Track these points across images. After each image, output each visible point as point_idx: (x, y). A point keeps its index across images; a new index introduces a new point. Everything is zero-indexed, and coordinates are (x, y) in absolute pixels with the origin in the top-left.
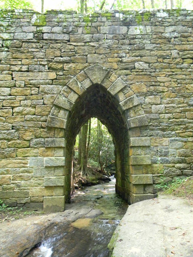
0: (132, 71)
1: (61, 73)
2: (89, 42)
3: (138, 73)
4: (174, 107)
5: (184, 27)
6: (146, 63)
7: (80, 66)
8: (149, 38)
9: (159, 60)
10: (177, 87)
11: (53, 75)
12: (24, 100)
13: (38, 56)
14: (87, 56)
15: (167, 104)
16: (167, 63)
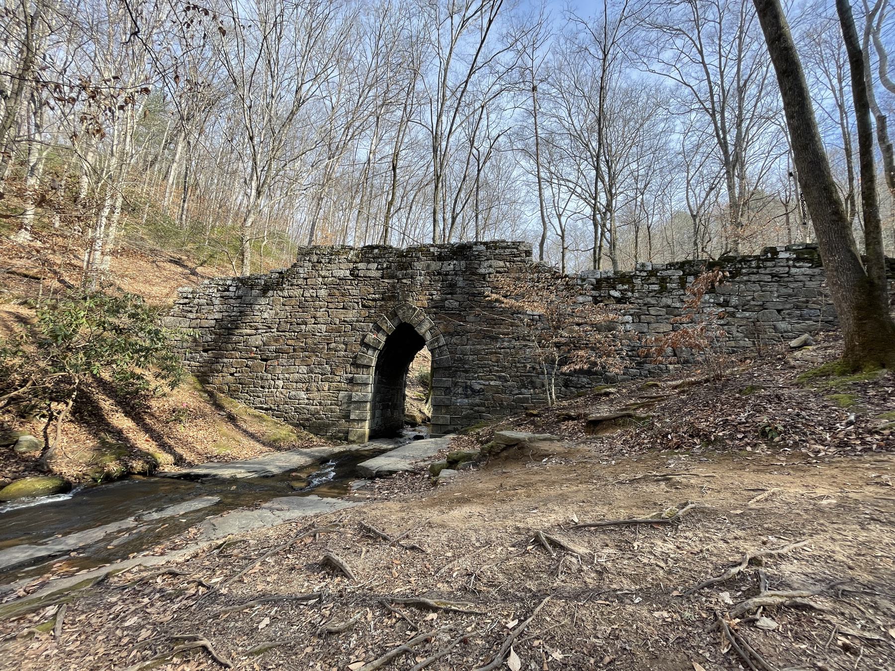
6: (457, 301)
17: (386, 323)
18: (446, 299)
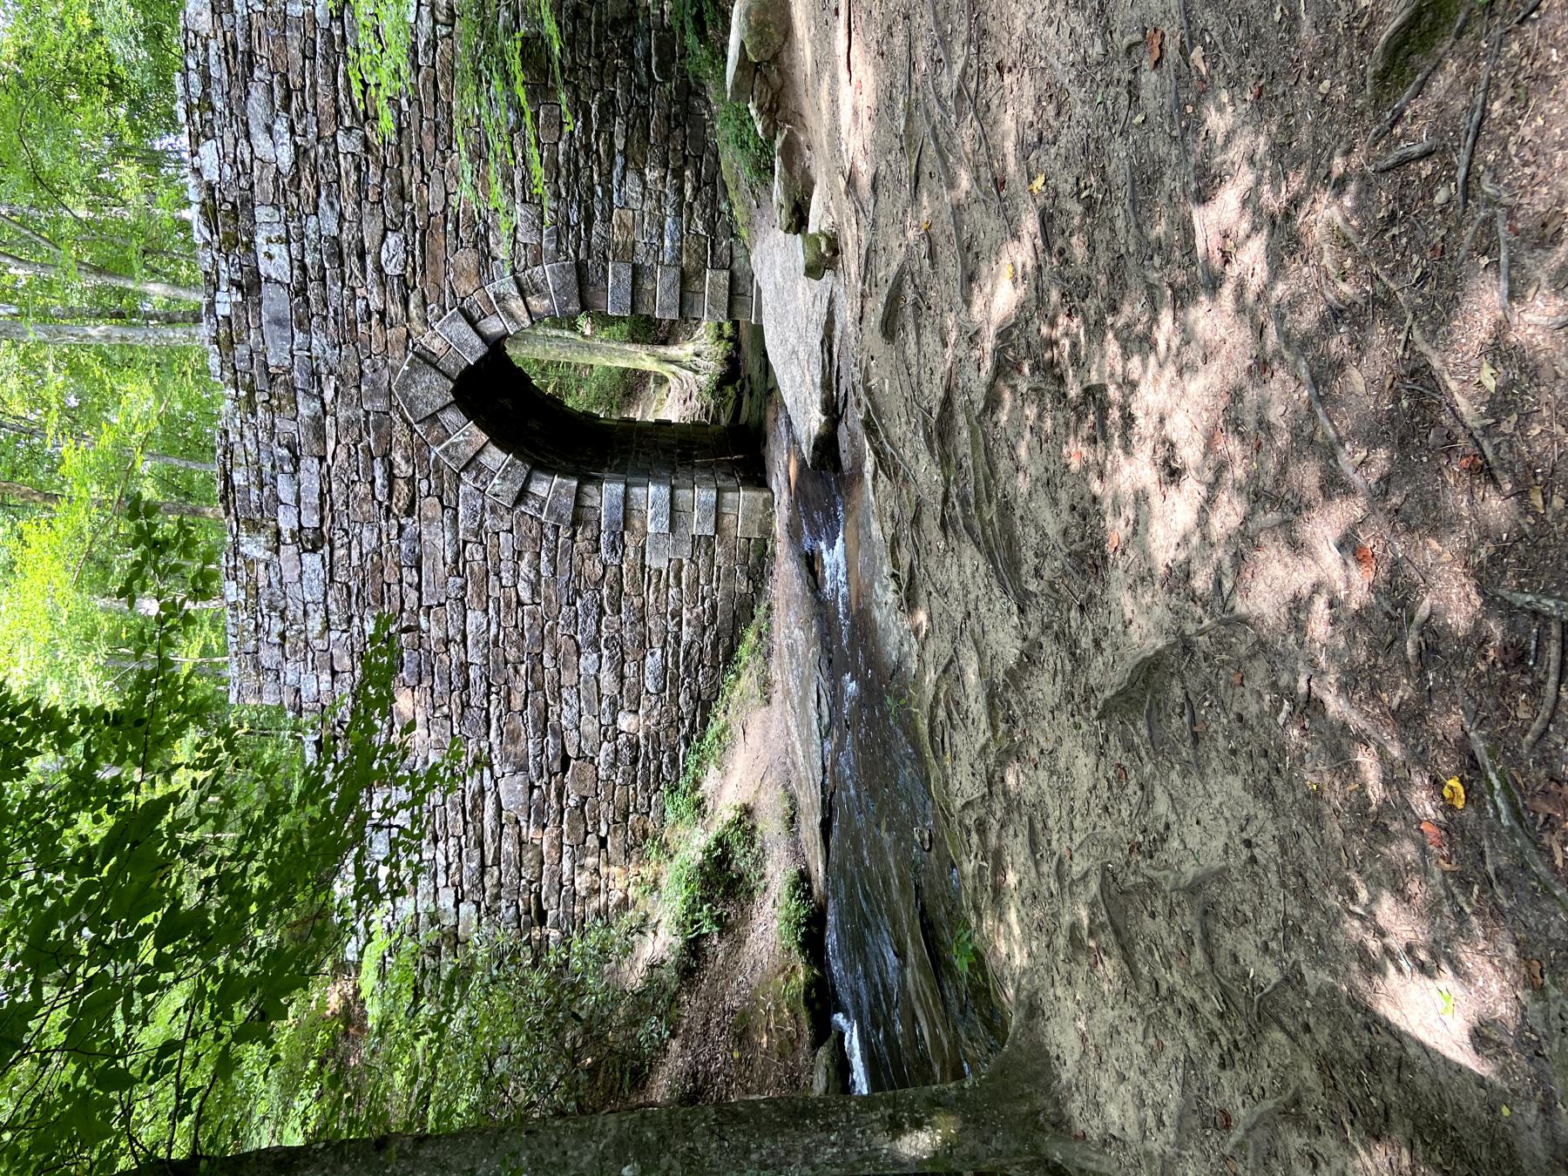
0: (411, 284)
1: (424, 484)
2: (323, 405)
5: (253, 91)
6: (384, 237)
7: (399, 429)
8: (300, 218)
11: (429, 506)
12: (500, 579)
13: (374, 543)
14: (367, 413)
16: (383, 172)
17: (455, 445)
18: (379, 269)
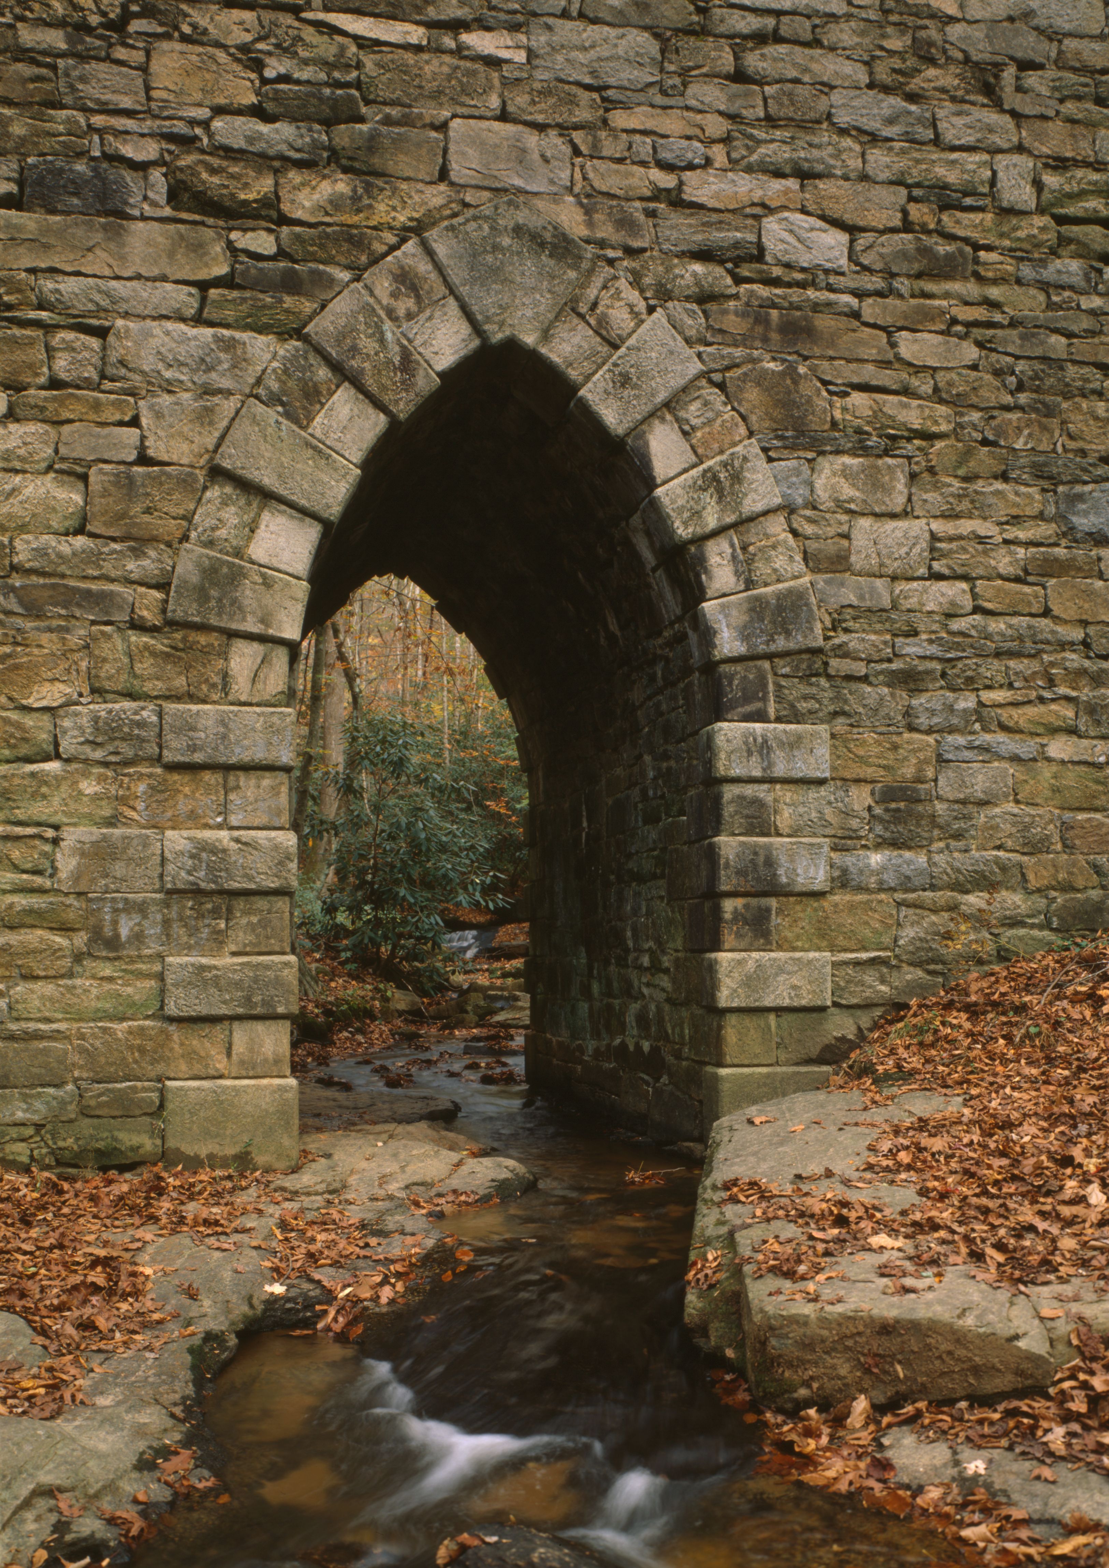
0: (745, 271)
3: (778, 291)
4: (981, 540)
9: (916, 212)
10: (1007, 408)
14: (443, 127)
15: (944, 516)
